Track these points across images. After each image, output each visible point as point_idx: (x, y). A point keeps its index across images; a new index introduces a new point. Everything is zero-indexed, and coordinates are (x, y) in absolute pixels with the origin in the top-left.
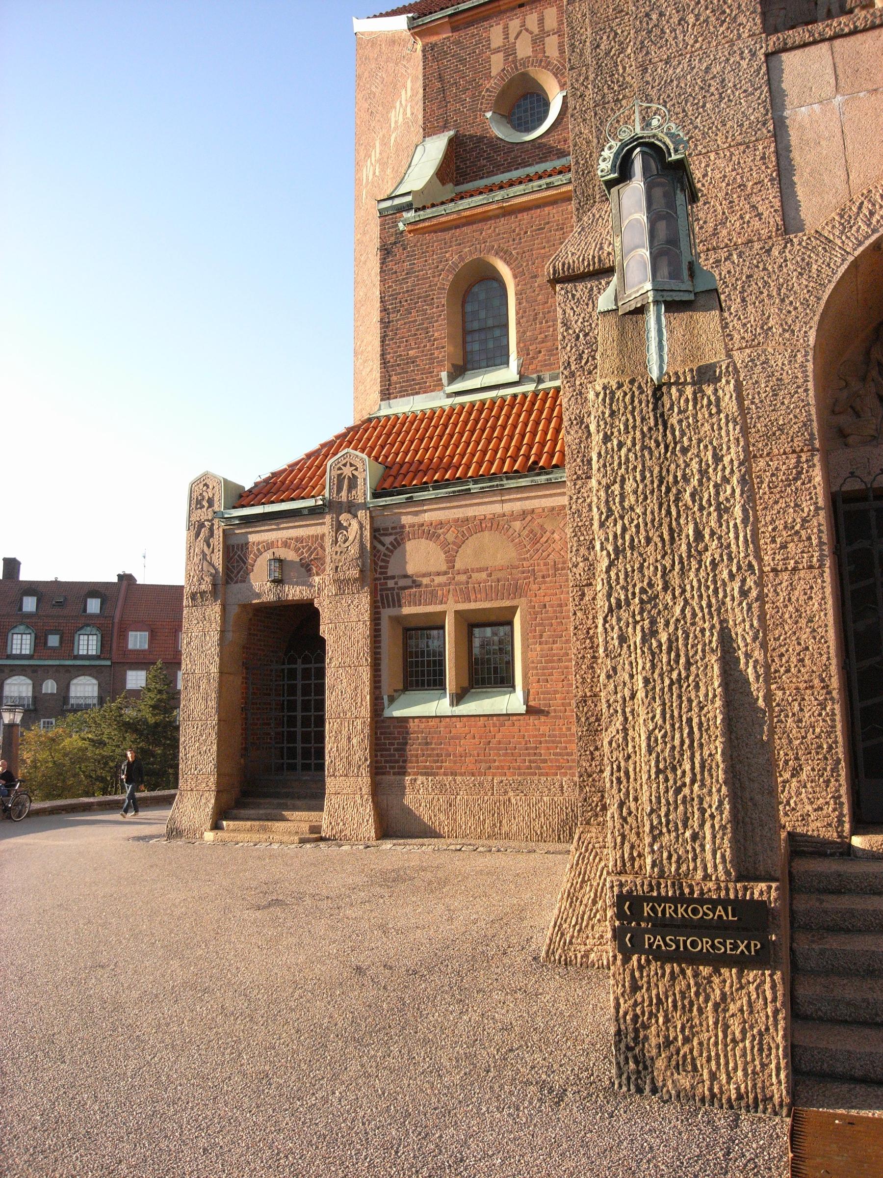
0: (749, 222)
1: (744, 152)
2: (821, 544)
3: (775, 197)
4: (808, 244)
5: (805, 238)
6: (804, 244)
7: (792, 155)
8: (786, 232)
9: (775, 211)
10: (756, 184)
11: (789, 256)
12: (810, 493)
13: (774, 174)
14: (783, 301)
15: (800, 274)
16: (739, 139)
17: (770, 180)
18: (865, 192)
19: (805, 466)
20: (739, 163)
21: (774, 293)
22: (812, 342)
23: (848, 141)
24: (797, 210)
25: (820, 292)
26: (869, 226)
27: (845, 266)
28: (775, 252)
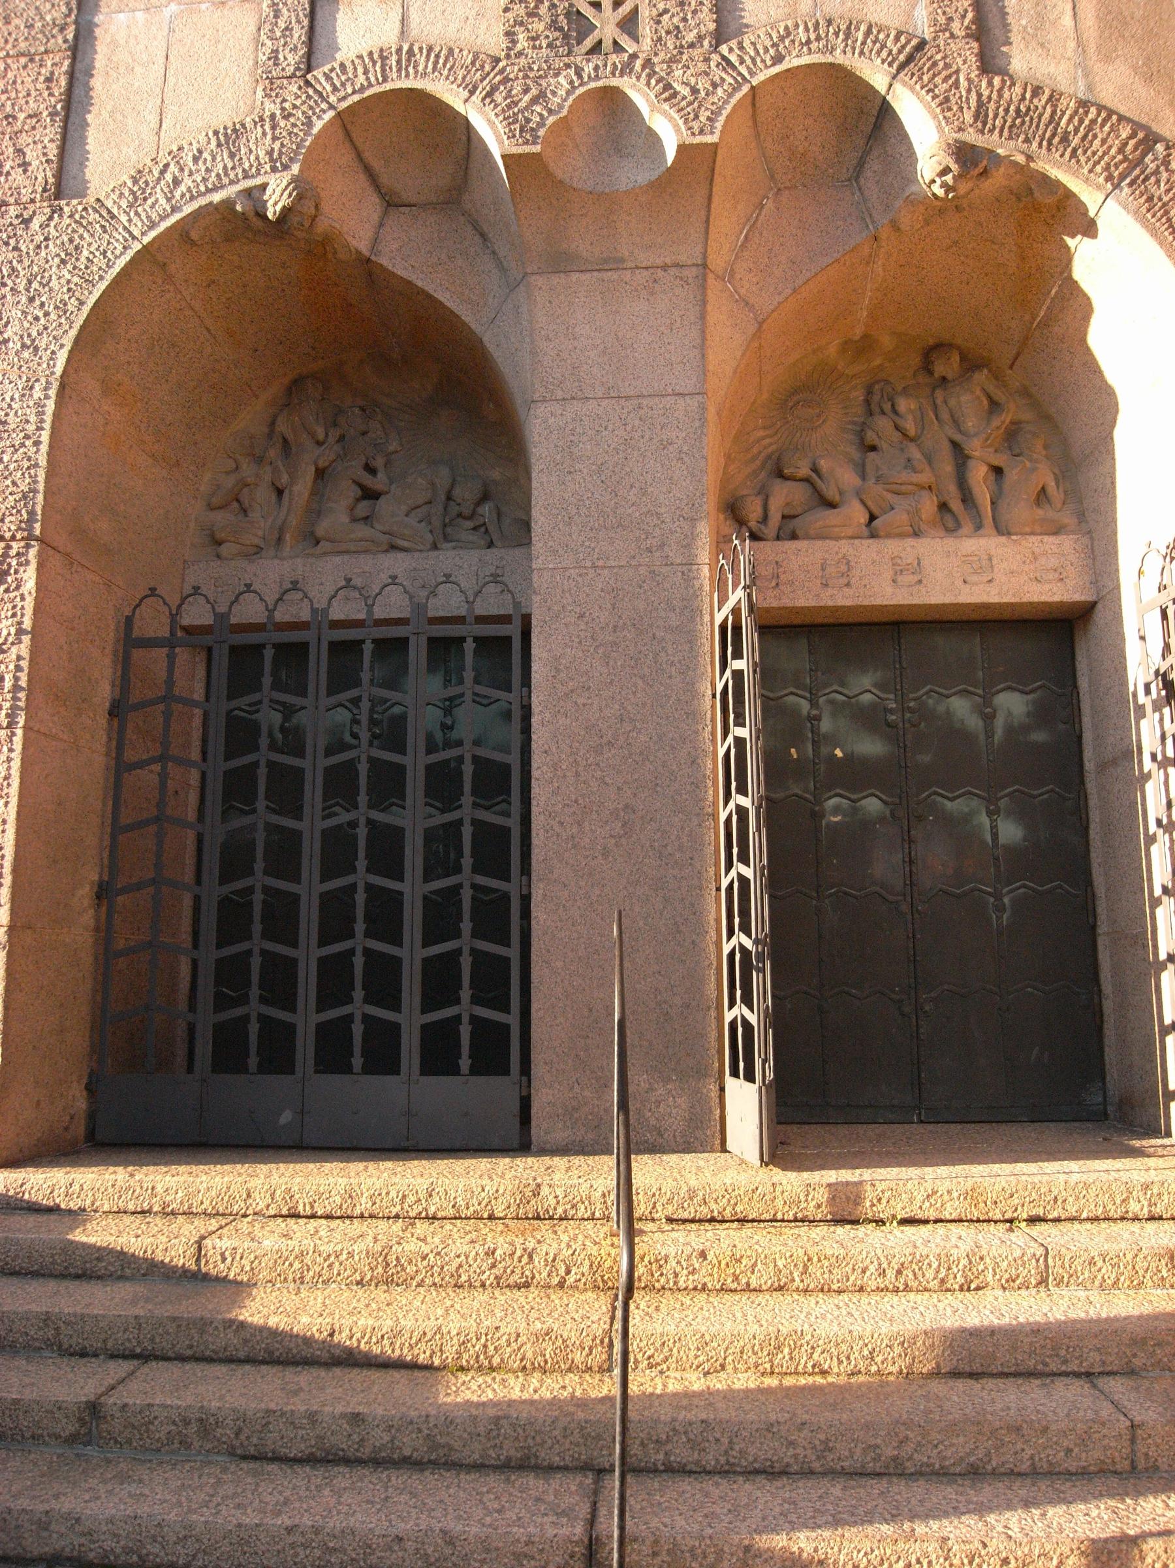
0: (8, 173)
1: (25, 67)
2: (16, 688)
3: (52, 141)
4: (82, 217)
5: (80, 208)
6: (77, 217)
7: (93, 82)
8: (58, 196)
9: (47, 161)
10: (30, 116)
11: (53, 233)
12: (14, 607)
13: (59, 107)
14: (31, 300)
15: (63, 262)
16: (23, 45)
17: (50, 114)
18: (175, 149)
19: (14, 562)
20: (14, 82)
21: (21, 288)
22: (59, 370)
23: (170, 73)
24: (82, 165)
25: (86, 292)
26: (168, 200)
27: (127, 257)
28: (35, 225)
